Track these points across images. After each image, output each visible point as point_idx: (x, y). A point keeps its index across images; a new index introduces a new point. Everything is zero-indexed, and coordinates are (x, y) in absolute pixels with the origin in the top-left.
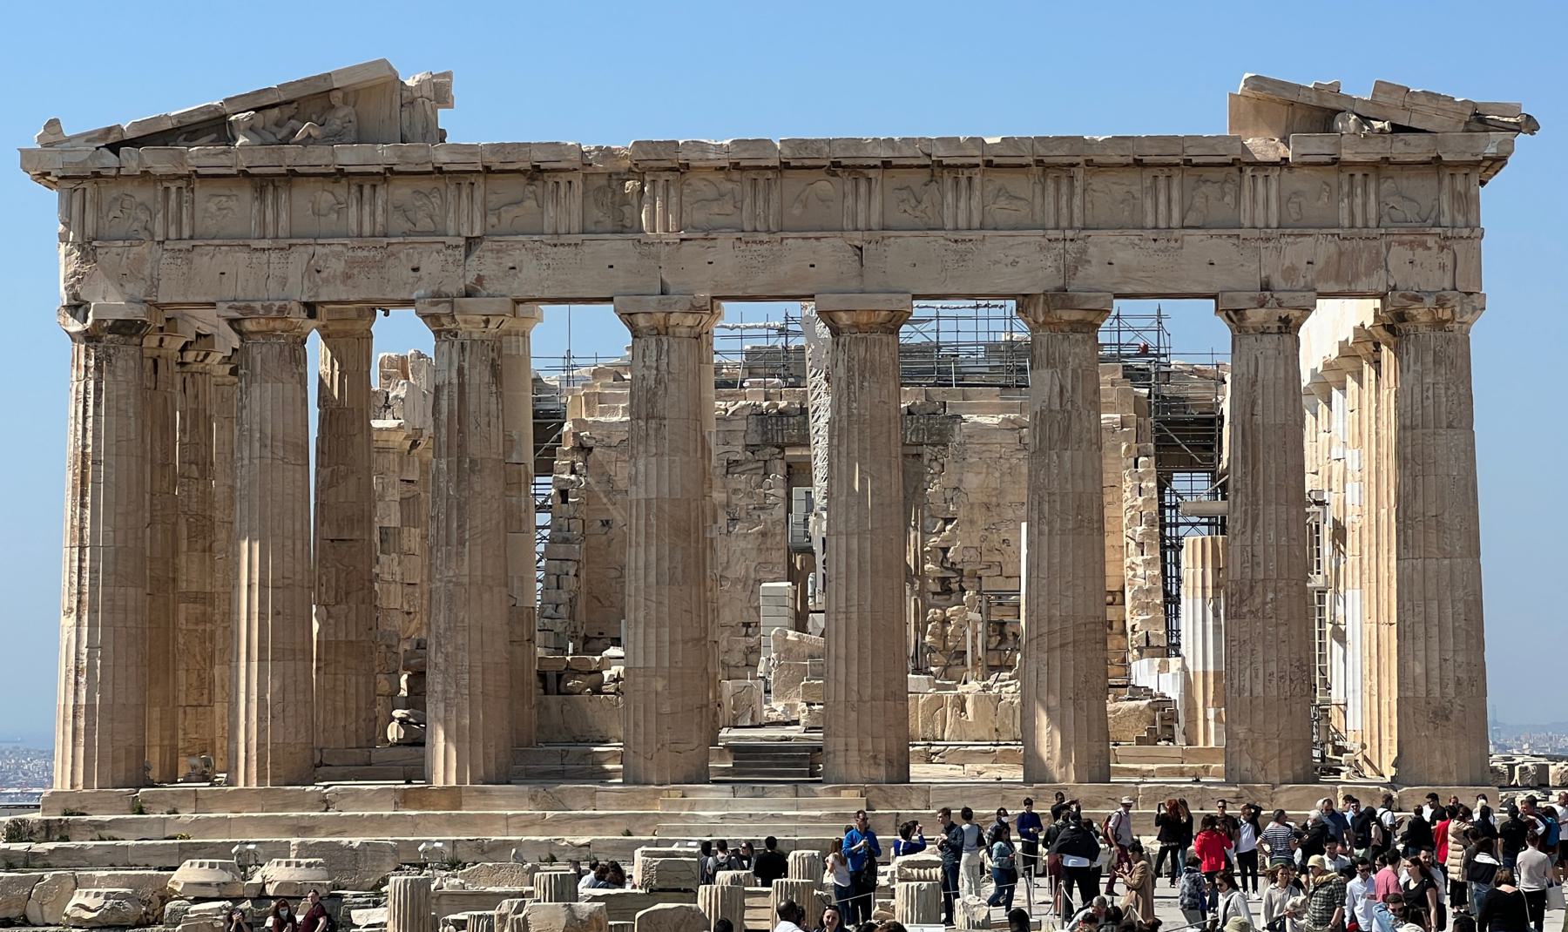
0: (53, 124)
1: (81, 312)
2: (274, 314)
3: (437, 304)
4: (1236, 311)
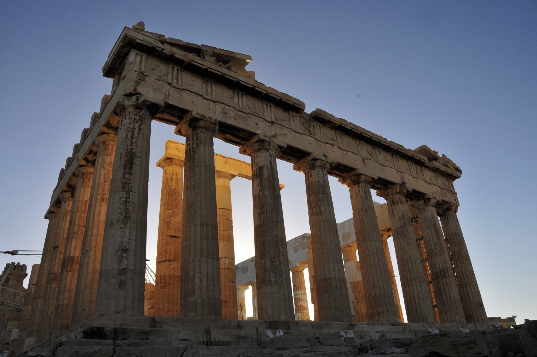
0: (142, 24)
1: (134, 98)
2: (213, 121)
3: (265, 137)
4: (429, 199)
